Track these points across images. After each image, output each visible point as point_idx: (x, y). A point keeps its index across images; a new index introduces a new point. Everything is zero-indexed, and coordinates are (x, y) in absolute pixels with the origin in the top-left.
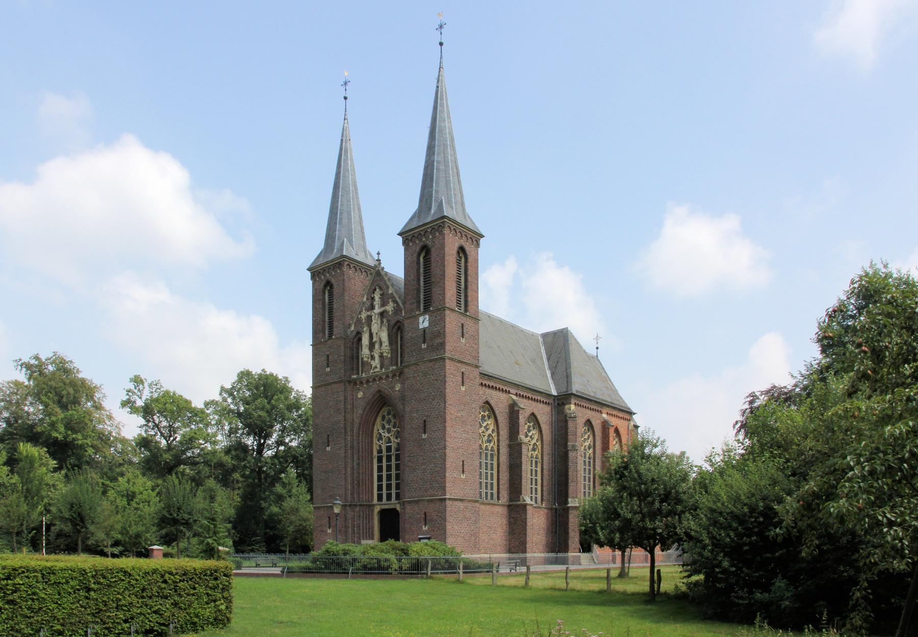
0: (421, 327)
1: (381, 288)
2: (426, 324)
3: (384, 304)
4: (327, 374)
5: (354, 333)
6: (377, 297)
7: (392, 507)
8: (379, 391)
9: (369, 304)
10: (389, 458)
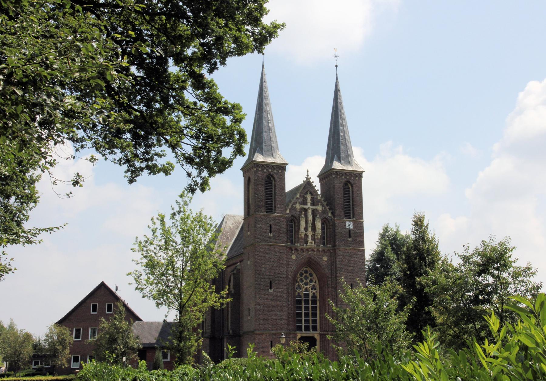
0: (348, 227)
1: (310, 193)
2: (351, 227)
3: (313, 204)
4: (270, 237)
5: (290, 215)
6: (309, 197)
7: (311, 335)
8: (310, 258)
9: (301, 200)
10: (307, 302)
